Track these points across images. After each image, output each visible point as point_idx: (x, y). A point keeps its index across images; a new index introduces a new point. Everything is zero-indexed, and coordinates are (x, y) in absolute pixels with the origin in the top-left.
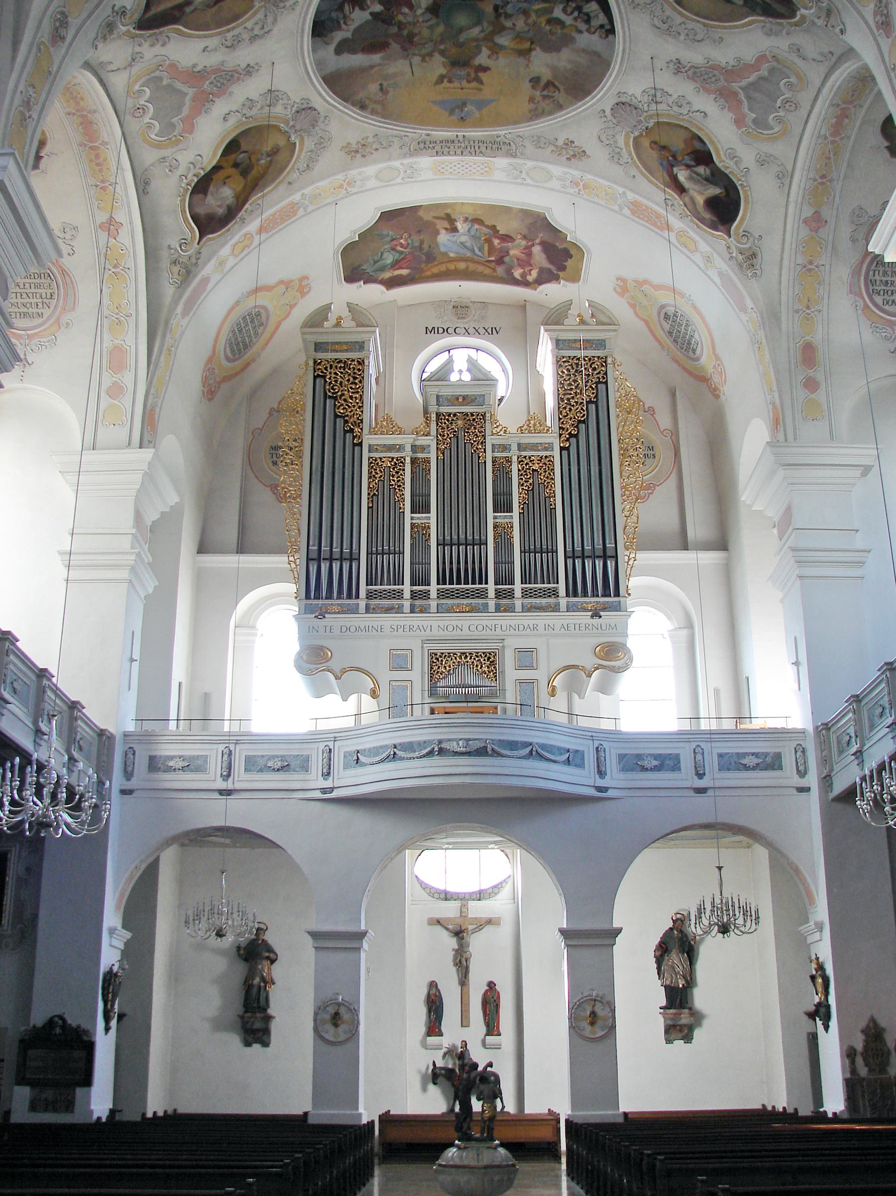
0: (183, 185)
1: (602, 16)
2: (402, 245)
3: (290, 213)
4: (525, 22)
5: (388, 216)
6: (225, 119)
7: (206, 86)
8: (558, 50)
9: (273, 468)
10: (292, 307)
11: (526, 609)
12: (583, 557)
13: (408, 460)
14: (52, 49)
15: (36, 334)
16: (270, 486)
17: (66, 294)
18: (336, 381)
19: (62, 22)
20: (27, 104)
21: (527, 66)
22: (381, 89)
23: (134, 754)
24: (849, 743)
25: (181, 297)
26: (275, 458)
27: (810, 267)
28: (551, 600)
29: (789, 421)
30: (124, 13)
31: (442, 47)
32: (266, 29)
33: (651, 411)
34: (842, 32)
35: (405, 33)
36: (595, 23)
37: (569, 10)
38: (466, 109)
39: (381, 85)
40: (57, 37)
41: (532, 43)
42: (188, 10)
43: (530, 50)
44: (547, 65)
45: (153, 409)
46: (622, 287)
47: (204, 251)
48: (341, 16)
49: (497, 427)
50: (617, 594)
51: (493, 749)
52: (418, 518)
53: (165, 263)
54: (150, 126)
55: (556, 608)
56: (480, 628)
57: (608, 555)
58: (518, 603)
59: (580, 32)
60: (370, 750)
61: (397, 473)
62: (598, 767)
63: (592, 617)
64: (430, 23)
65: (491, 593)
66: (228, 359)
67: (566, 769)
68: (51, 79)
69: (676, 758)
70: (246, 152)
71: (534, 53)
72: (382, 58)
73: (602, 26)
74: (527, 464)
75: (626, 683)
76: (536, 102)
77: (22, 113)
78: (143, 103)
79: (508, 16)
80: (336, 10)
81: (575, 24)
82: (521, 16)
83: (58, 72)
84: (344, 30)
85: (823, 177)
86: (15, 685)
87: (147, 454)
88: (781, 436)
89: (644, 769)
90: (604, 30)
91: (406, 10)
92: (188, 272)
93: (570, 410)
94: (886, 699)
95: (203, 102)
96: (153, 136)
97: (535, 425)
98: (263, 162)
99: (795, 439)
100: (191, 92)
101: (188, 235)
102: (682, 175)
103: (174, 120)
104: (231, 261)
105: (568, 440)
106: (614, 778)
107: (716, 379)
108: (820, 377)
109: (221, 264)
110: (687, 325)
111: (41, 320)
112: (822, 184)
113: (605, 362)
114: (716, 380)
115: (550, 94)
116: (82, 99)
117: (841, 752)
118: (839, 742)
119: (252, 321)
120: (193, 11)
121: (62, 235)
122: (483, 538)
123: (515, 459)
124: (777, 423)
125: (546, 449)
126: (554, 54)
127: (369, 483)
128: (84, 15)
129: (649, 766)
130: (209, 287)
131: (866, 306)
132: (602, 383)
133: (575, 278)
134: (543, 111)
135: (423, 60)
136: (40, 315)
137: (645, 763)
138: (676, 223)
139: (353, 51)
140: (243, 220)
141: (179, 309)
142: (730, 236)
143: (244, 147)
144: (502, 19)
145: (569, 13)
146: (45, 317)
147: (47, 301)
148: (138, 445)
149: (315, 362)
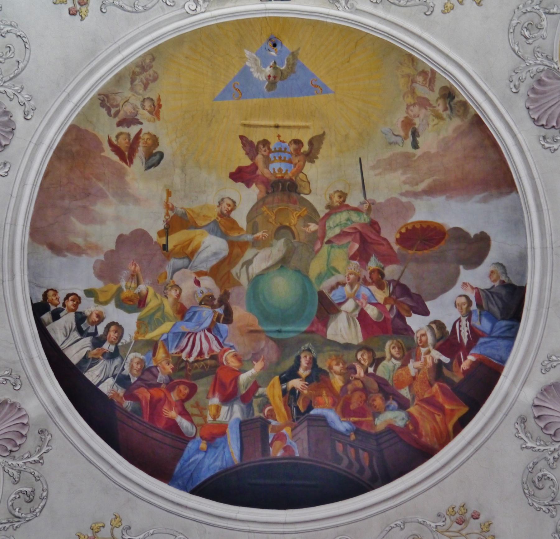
1: (59, 337)
4: (181, 290)
8: (121, 240)
21: (169, 194)
22: (415, 134)
31: (313, 227)
35: (373, 263)
37: (112, 335)
38: (268, 70)
39: (415, 145)
41: (165, 247)
43: (167, 231)
44: (137, 201)
48: (475, 318)
59: (89, 293)
64: (332, 281)
71: (161, 226)
72: (410, 209)
73: (56, 316)
76: (147, 104)
79: (208, 300)
80: (483, 334)
81: (101, 308)
82: (187, 304)
84: (472, 288)
90: (53, 308)
91: (372, 312)
115: (124, 129)
126: (127, 230)
134: (133, 81)
135: (343, 195)
144: (217, 293)
145: (113, 328)
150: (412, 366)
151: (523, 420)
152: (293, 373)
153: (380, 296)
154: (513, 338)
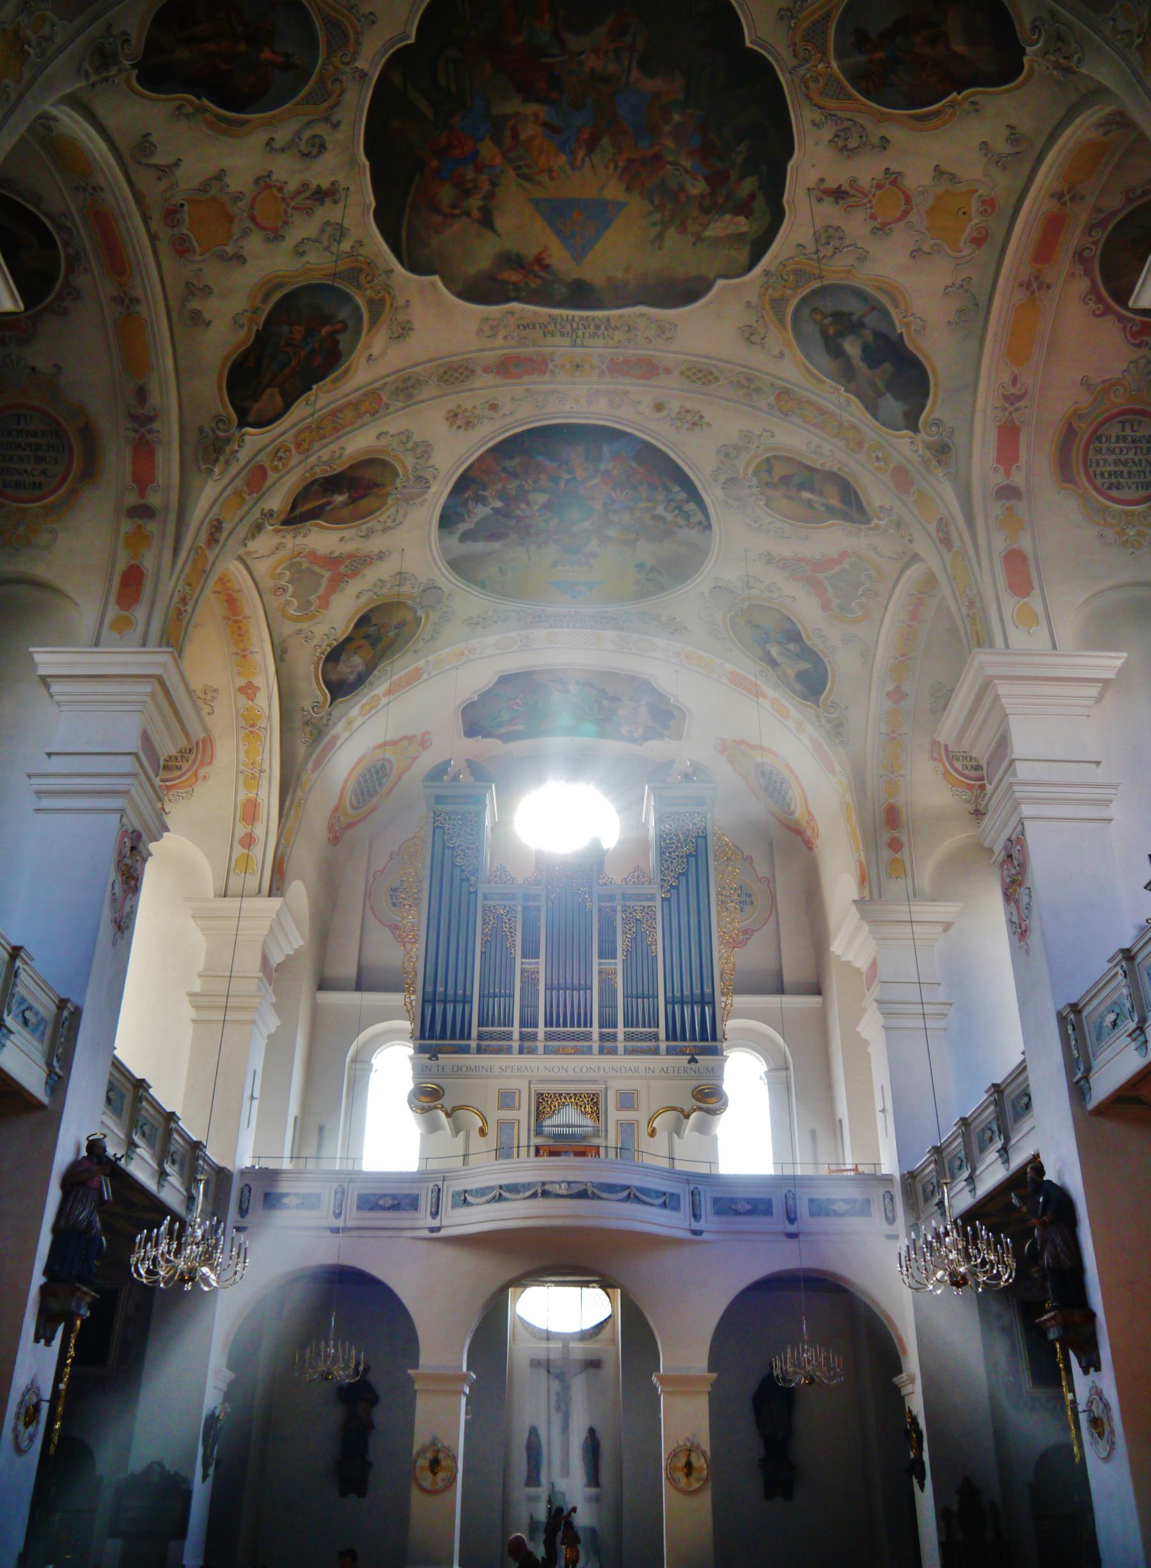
0: (317, 654)
2: (518, 705)
3: (415, 676)
5: (505, 680)
6: (358, 597)
7: (342, 569)
9: (393, 909)
10: (415, 759)
11: (629, 1052)
12: (682, 1003)
13: (520, 908)
14: (207, 551)
15: (173, 785)
16: (389, 926)
17: (204, 750)
18: (454, 832)
19: (217, 526)
20: (184, 600)
23: (250, 1191)
24: (933, 1193)
25: (312, 753)
26: (394, 900)
27: (893, 735)
28: (652, 1044)
29: (874, 876)
30: (271, 515)
32: (397, 522)
33: (750, 859)
34: (910, 541)
36: (694, 520)
39: (501, 568)
40: (213, 540)
42: (328, 508)
45: (282, 858)
46: (723, 747)
47: (335, 713)
49: (603, 878)
50: (714, 1039)
51: (593, 1193)
52: (529, 964)
53: (298, 723)
54: (288, 603)
55: (656, 1051)
56: (584, 1070)
57: (706, 1000)
58: (621, 1046)
59: (681, 527)
60: (477, 1190)
61: (509, 920)
62: (693, 1209)
63: (689, 1062)
65: (596, 1036)
66: (353, 807)
67: (663, 1212)
68: (204, 576)
69: (769, 1203)
70: (375, 625)
73: (700, 523)
74: (630, 913)
75: (725, 1126)
77: (179, 610)
78: (283, 583)
83: (211, 569)
85: (902, 655)
86: (146, 1128)
87: (277, 902)
88: (866, 893)
89: (737, 1213)
91: (523, 506)
92: (320, 732)
93: (672, 863)
94: (963, 1152)
95: (337, 582)
96: (292, 612)
97: (638, 877)
98: (391, 633)
99: (880, 896)
100: (327, 574)
101: (321, 699)
102: (774, 651)
103: (312, 598)
104: (360, 721)
105: (669, 891)
106: (709, 1222)
107: (809, 832)
108: (904, 838)
109: (350, 723)
110: (782, 783)
111: (178, 773)
112: (902, 662)
113: (705, 818)
114: (809, 834)
116: (229, 581)
117: (926, 1200)
118: (924, 1190)
119: (377, 773)
120: (332, 509)
121: (203, 696)
122: (588, 983)
123: (619, 908)
124: (863, 879)
125: (648, 900)
127: (483, 929)
128: (237, 519)
129: (742, 1210)
130: (338, 744)
131: (946, 770)
132: (702, 837)
133: (678, 736)
136: (179, 768)
137: (739, 1207)
138: (770, 692)
139: (475, 540)
140: (371, 684)
141: (310, 765)
142: (818, 707)
143: (374, 621)
146: (183, 770)
147: (186, 755)
148: (267, 893)
149: (435, 813)
150: (500, 486)
151: (435, 478)
152: (568, 481)
153: (519, 512)
154: (444, 508)
